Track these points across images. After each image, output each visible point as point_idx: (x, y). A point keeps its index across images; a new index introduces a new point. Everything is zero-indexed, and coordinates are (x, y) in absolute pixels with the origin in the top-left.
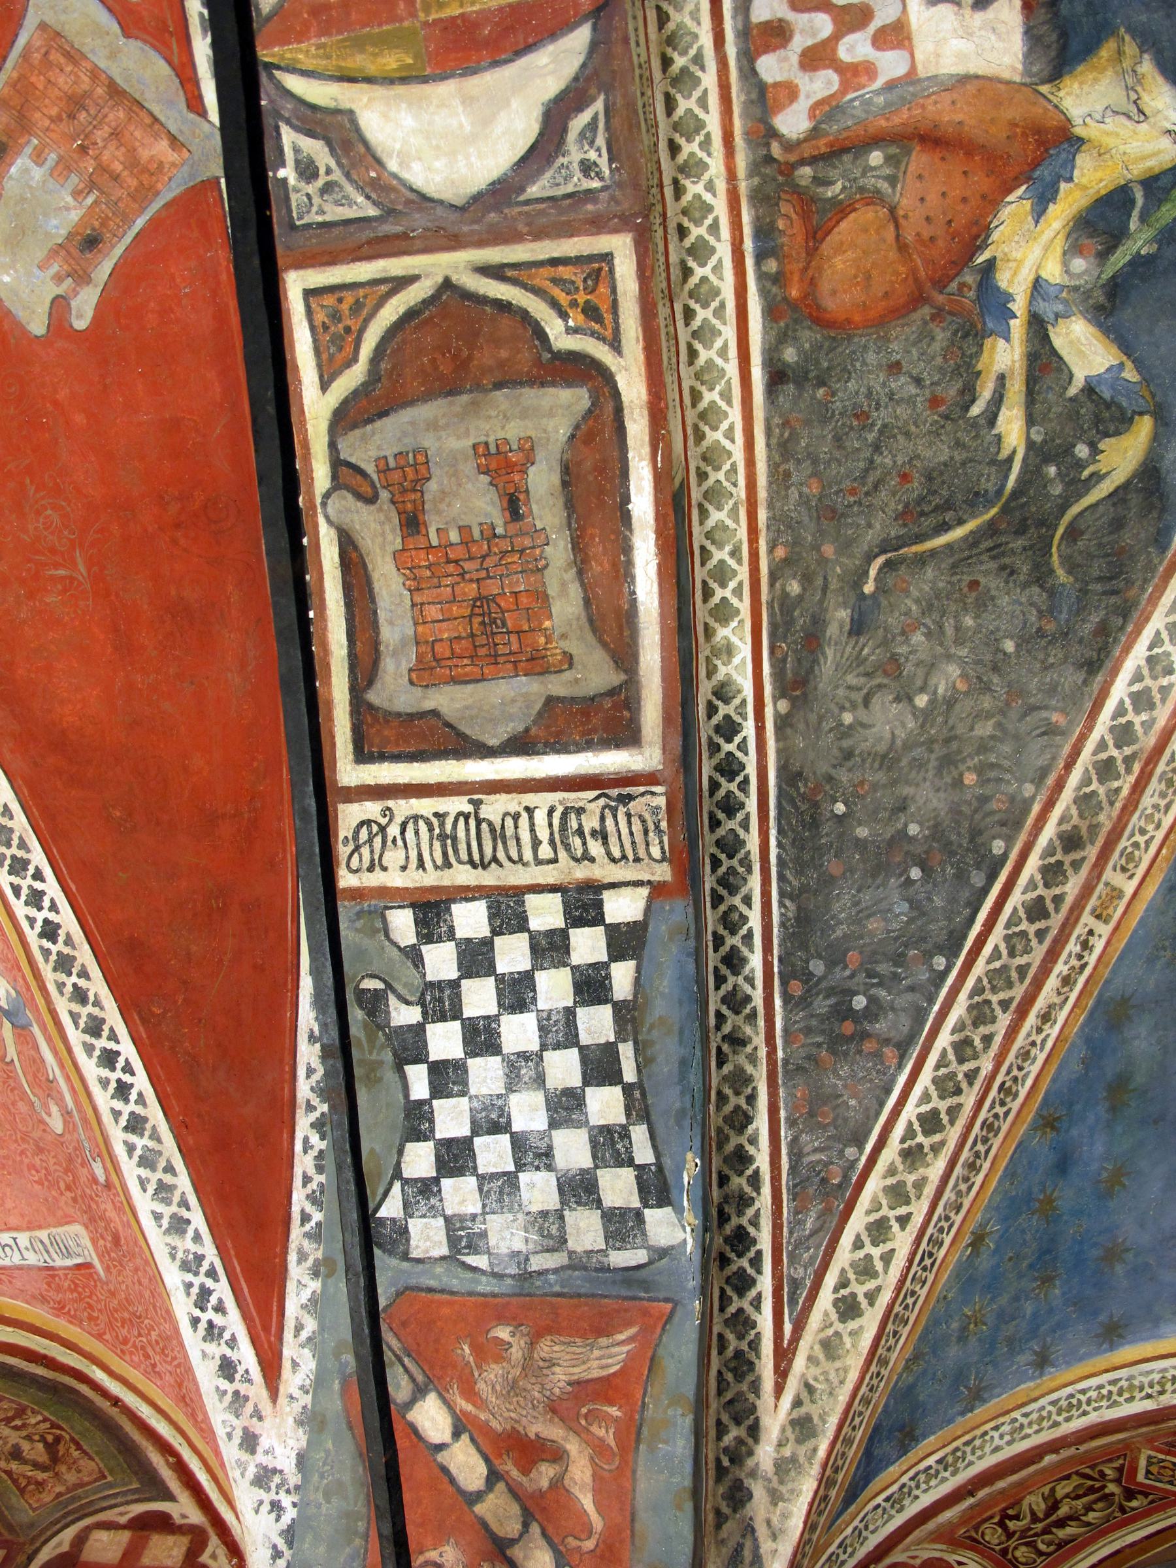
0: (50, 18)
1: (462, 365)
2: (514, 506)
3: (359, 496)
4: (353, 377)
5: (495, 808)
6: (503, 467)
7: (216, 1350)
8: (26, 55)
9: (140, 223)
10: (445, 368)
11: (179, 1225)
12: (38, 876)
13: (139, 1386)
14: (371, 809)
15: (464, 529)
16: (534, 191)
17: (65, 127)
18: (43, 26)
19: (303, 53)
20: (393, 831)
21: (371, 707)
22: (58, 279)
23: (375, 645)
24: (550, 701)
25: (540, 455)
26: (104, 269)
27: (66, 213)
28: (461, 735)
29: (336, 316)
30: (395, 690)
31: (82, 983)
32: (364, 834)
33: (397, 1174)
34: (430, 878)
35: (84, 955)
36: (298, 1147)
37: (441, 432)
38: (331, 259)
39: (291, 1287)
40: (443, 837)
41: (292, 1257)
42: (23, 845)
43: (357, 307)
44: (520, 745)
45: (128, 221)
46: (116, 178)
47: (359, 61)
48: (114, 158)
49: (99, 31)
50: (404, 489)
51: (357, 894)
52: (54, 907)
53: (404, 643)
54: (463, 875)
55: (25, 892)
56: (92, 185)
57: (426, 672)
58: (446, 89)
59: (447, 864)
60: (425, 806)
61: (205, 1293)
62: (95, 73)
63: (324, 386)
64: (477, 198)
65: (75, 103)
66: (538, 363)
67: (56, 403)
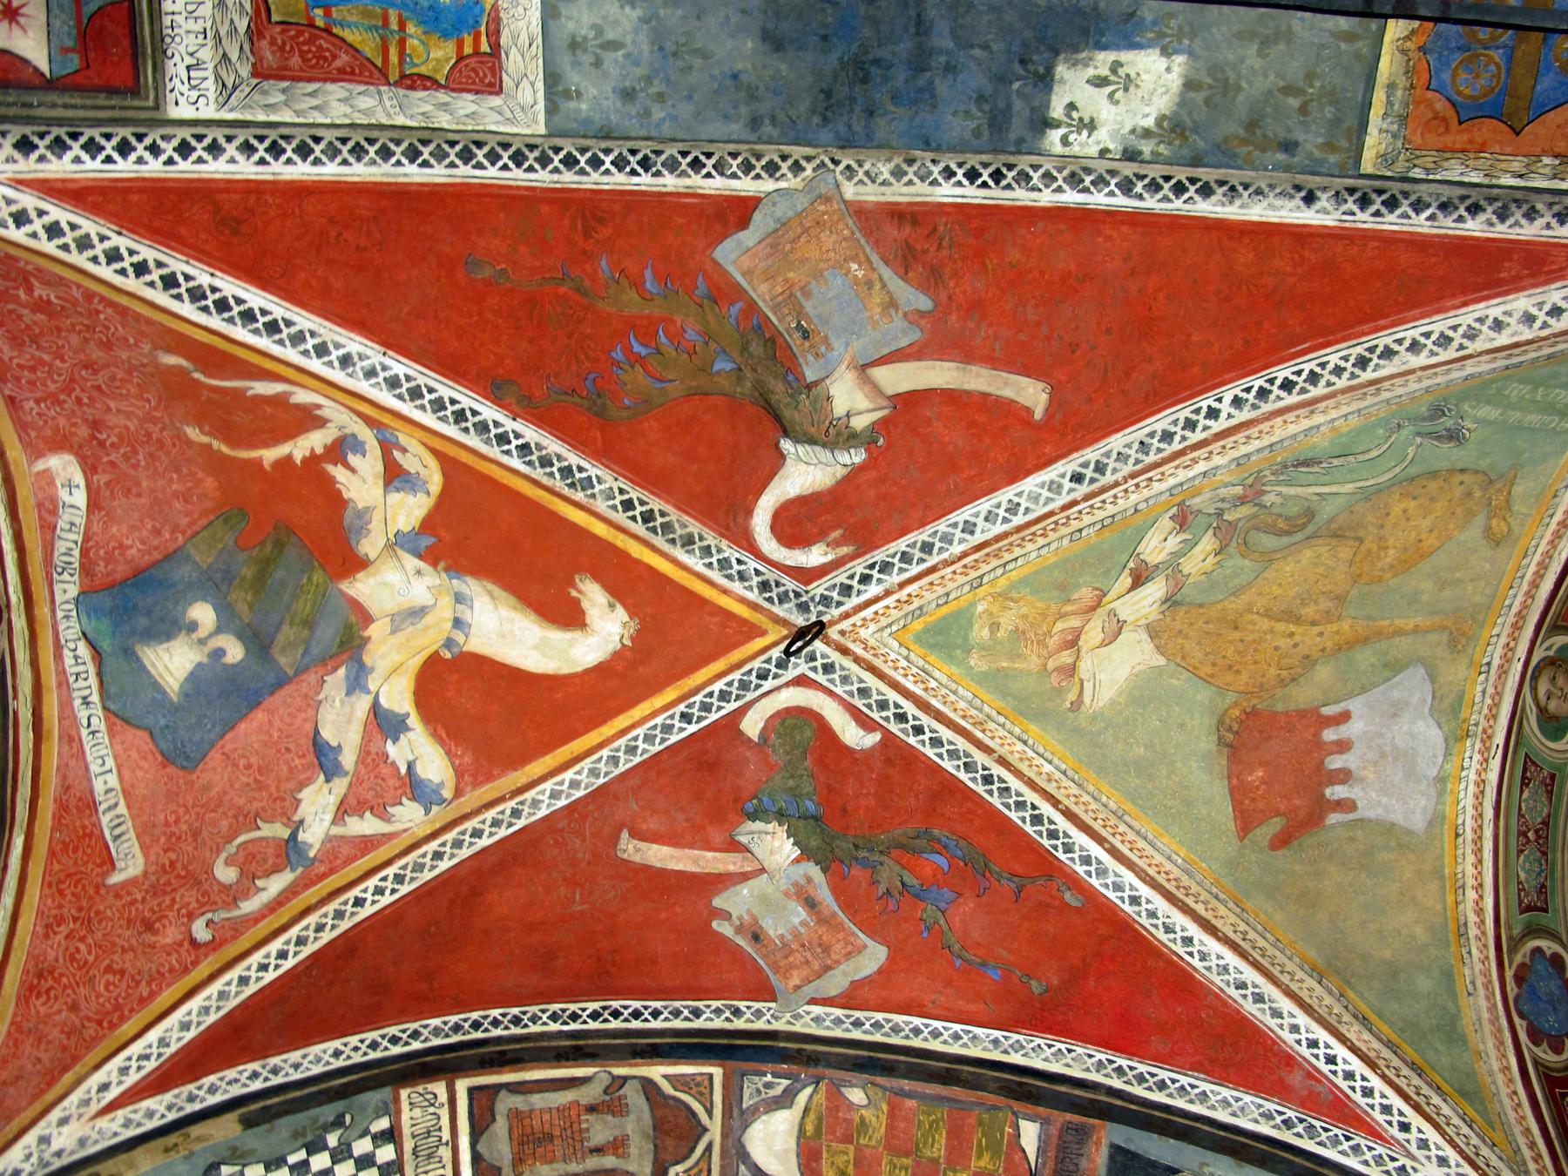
0: (868, 951)
1: (667, 1133)
2: (598, 1150)
3: (608, 1087)
4: (667, 1088)
5: (445, 1153)
6: (618, 1146)
7: (114, 1077)
8: (854, 934)
9: (761, 962)
10: (667, 1127)
11: (185, 1026)
12: (393, 891)
13: (26, 899)
14: (443, 1097)
15: (588, 1130)
16: (742, 1168)
17: (816, 941)
18: (865, 946)
19: (821, 1098)
20: (432, 1110)
21: (497, 1093)
22: (740, 918)
23: (531, 1092)
24: (499, 1169)
25: (621, 1161)
26: (741, 941)
27: (774, 929)
28: (482, 1133)
29: (698, 1085)
30: (505, 1103)
31: (328, 927)
32: (429, 1096)
33: (244, 1166)
34: (406, 1131)
35: (345, 925)
36: (240, 1068)
37: (637, 1120)
38: (725, 1087)
39: (159, 1098)
40: (429, 1132)
41: (176, 1091)
42: (412, 879)
43: (702, 1094)
44: (476, 1158)
45: (764, 957)
46: (786, 957)
47: (812, 1116)
48: (797, 958)
49: (857, 970)
50: (612, 1104)
51: (397, 1100)
52: (374, 902)
53: (531, 1104)
54: (408, 1145)
55: (383, 884)
56: (785, 945)
57: (515, 1115)
58: (793, 1145)
59: (414, 1136)
60: (445, 1122)
61: (147, 1057)
62: (838, 963)
63: (665, 1076)
64: (743, 1147)
65: (826, 949)
66: (664, 1161)
67: (674, 905)
